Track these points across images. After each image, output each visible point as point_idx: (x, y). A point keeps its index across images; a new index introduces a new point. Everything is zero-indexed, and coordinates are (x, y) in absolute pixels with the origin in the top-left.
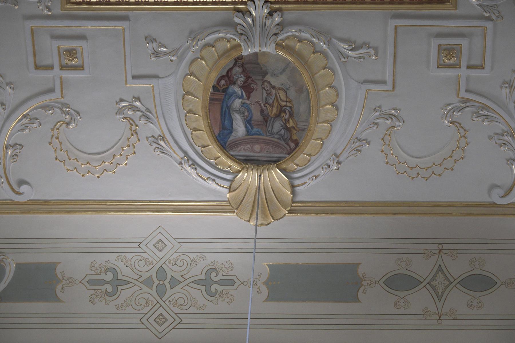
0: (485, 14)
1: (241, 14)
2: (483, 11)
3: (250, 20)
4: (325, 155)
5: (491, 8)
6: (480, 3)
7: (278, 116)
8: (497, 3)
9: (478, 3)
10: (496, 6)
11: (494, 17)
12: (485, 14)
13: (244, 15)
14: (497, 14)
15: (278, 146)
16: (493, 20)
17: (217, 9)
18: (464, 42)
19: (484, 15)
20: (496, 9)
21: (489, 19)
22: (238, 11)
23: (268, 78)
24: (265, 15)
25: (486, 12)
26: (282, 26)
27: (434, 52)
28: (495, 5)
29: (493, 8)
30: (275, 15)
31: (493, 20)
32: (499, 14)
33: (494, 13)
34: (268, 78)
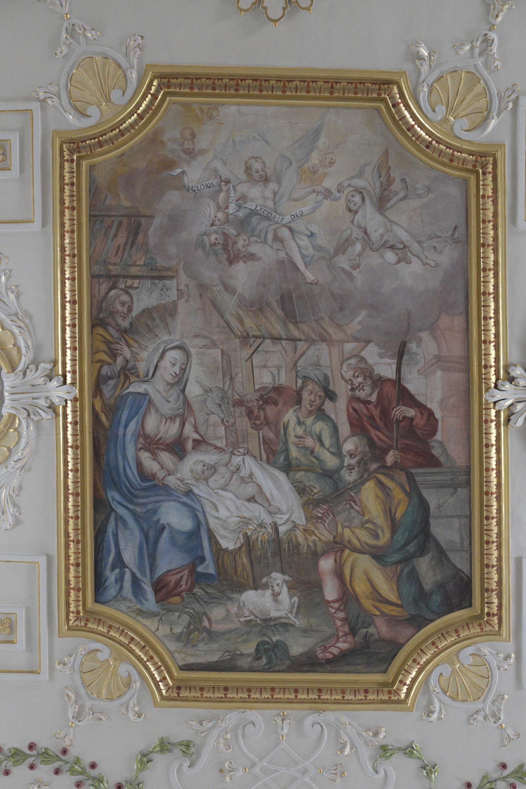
0: (509, 109)
1: (512, 418)
2: (505, 111)
3: (519, 407)
5: (502, 101)
6: (496, 115)
8: (496, 92)
9: (495, 117)
10: (500, 95)
11: (514, 96)
12: (509, 109)
13: (513, 414)
14: (510, 93)
16: (517, 98)
17: (506, 446)
19: (511, 109)
20: (503, 95)
21: (516, 102)
22: (508, 420)
24: (513, 386)
25: (508, 107)
28: (498, 95)
29: (502, 98)
30: (513, 374)
31: (517, 98)
32: (510, 90)
33: (509, 97)
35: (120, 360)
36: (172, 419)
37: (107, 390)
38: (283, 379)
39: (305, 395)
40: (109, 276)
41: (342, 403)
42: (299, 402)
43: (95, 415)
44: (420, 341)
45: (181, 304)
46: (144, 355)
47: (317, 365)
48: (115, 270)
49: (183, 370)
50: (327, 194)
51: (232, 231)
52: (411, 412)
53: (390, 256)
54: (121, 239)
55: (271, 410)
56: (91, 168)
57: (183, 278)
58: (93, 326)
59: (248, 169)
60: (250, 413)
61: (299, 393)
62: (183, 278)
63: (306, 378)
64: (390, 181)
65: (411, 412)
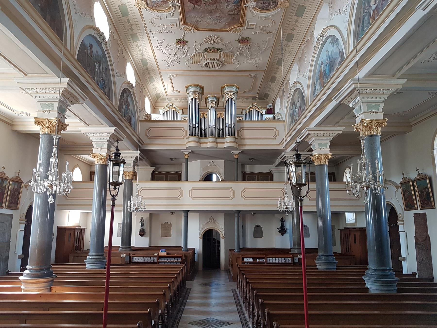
4: (151, 12)
7: (157, 6)
15: (151, 6)
18: (176, 26)
23: (164, 4)
26: (175, 7)
27: (173, 23)
34: (164, 4)
35: (237, 7)
36: (229, 1)
37: (239, 4)
38: (212, 5)
39: (208, 4)
40: (238, 15)
41: (203, 3)
42: (209, 3)
43: (241, 2)
44: (191, 9)
45: (227, 12)
46: (233, 8)
47: (207, 7)
48: (237, 15)
49: (227, 6)
50: (205, 22)
51: (219, 19)
52: (192, 2)
53: (196, 16)
54: (235, 18)
55: (214, 2)
56: (239, 24)
57: (227, 15)
58: (241, 10)
59: (217, 24)
60: (217, 2)
61: (209, 4)
62: (227, 15)
63: (208, 5)
64: (197, 22)
65: (192, 2)
